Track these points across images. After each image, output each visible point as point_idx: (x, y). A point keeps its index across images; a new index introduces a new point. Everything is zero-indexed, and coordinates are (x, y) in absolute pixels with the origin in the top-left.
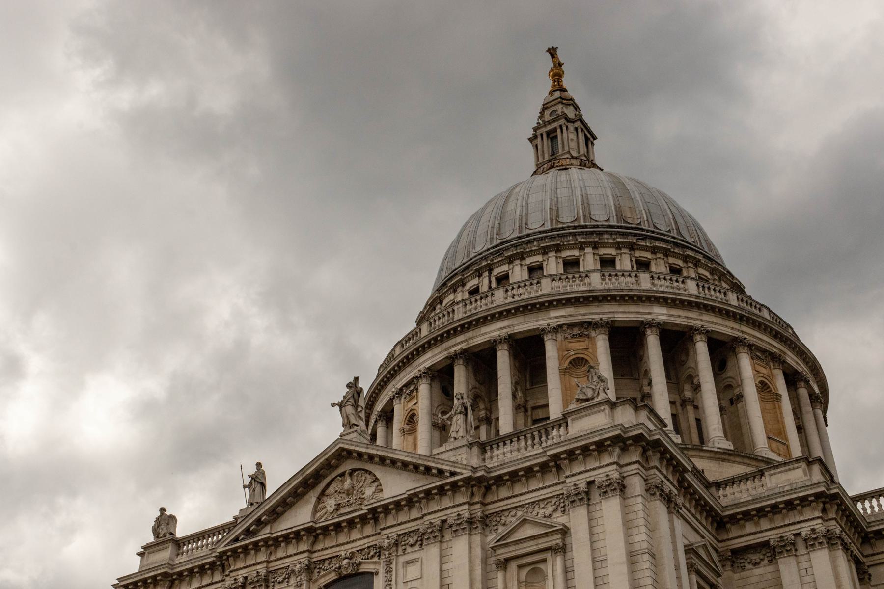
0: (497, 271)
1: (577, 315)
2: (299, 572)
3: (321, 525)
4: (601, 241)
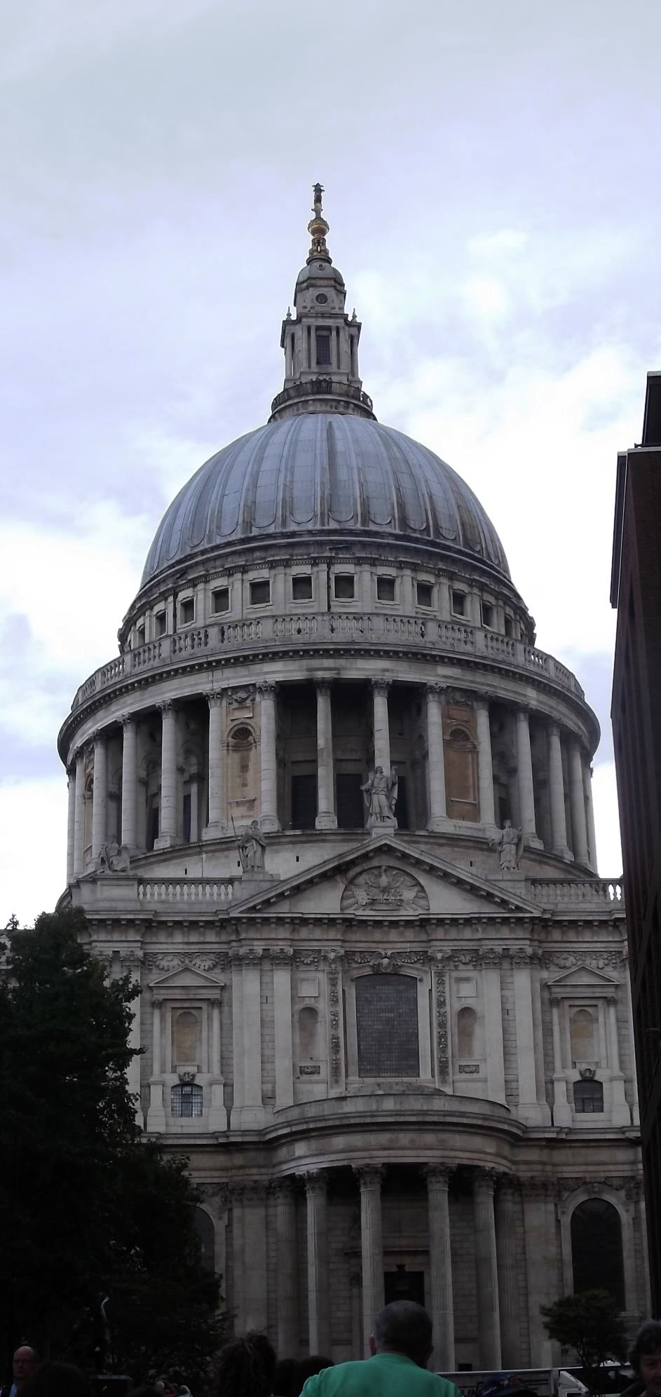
0: (339, 569)
1: (463, 680)
2: (333, 960)
3: (361, 918)
4: (459, 573)
